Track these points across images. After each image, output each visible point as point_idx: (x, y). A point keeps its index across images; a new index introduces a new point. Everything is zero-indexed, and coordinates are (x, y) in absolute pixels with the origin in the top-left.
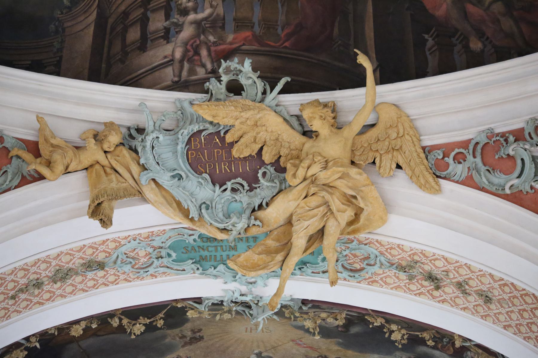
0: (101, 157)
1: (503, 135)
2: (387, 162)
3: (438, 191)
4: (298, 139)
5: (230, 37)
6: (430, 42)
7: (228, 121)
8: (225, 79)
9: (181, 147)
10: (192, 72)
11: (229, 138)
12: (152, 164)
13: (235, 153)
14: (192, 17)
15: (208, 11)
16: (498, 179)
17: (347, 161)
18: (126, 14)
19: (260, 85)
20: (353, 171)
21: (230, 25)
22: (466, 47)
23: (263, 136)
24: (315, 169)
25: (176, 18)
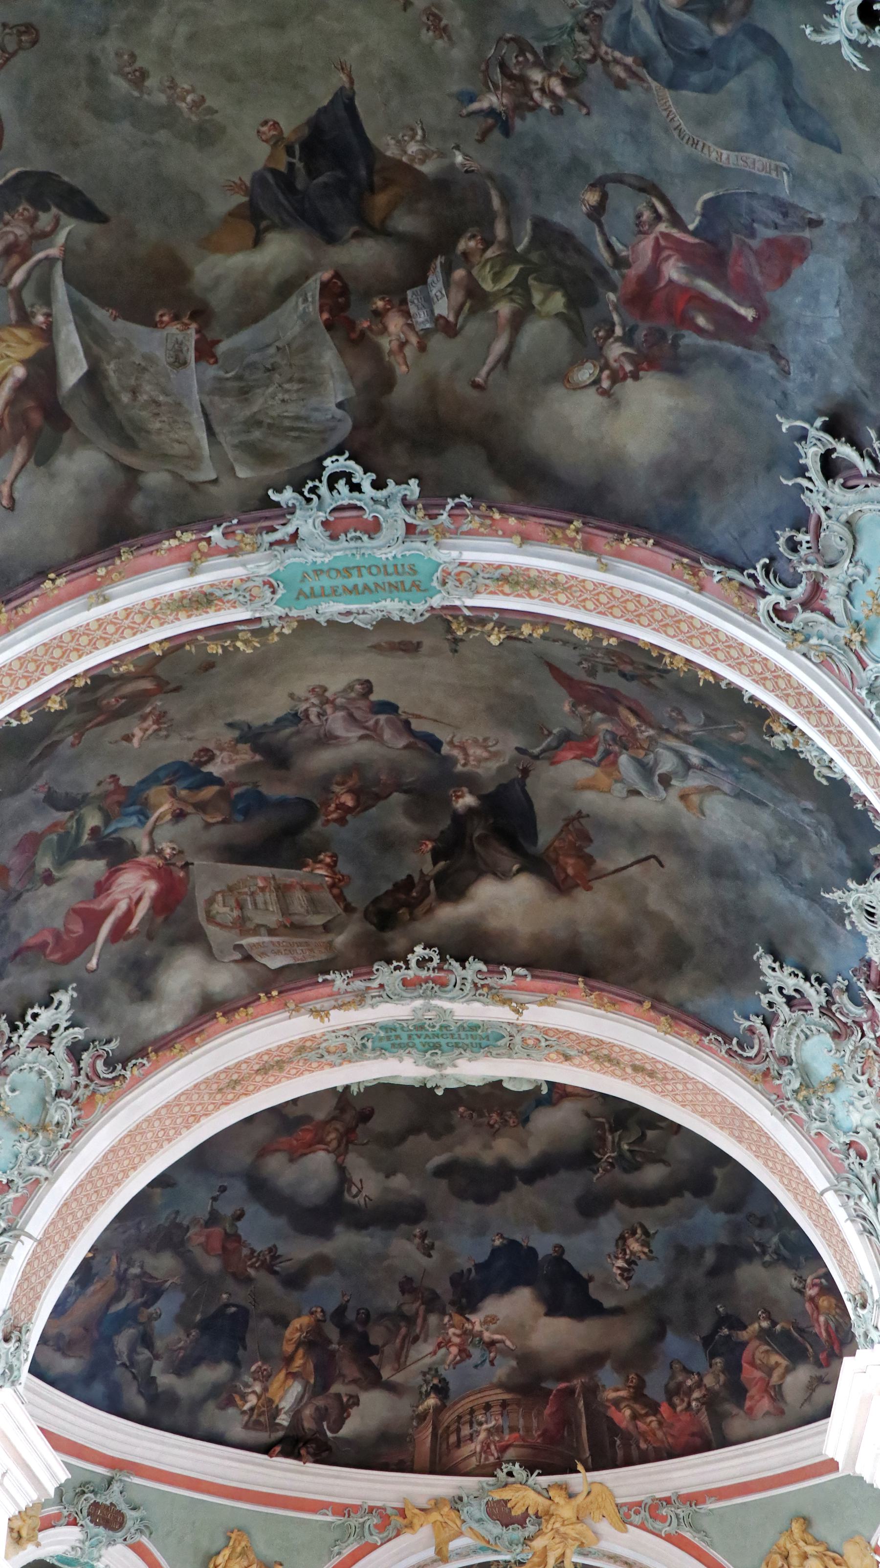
0: (440, 1518)
1: (660, 1499)
2: (597, 1514)
3: (626, 1531)
4: (548, 1502)
5: (507, 1438)
6: (618, 1442)
7: (508, 1498)
8: (505, 1471)
9: (483, 1507)
10: (486, 1459)
11: (509, 1505)
12: (467, 1519)
13: (513, 1513)
14: (485, 1426)
15: (493, 1423)
16: (658, 1525)
17: (574, 1520)
18: (448, 1427)
19: (524, 1474)
20: (579, 1527)
21: (506, 1431)
22: (638, 1447)
23: (527, 1503)
24: (557, 1525)
25: (476, 1427)
